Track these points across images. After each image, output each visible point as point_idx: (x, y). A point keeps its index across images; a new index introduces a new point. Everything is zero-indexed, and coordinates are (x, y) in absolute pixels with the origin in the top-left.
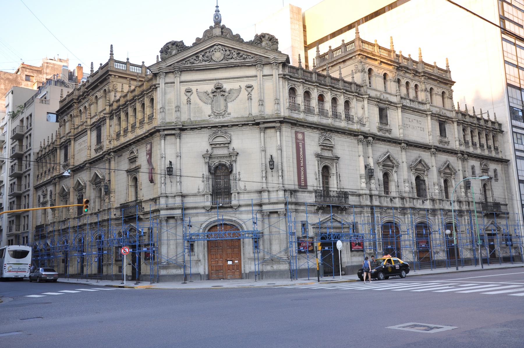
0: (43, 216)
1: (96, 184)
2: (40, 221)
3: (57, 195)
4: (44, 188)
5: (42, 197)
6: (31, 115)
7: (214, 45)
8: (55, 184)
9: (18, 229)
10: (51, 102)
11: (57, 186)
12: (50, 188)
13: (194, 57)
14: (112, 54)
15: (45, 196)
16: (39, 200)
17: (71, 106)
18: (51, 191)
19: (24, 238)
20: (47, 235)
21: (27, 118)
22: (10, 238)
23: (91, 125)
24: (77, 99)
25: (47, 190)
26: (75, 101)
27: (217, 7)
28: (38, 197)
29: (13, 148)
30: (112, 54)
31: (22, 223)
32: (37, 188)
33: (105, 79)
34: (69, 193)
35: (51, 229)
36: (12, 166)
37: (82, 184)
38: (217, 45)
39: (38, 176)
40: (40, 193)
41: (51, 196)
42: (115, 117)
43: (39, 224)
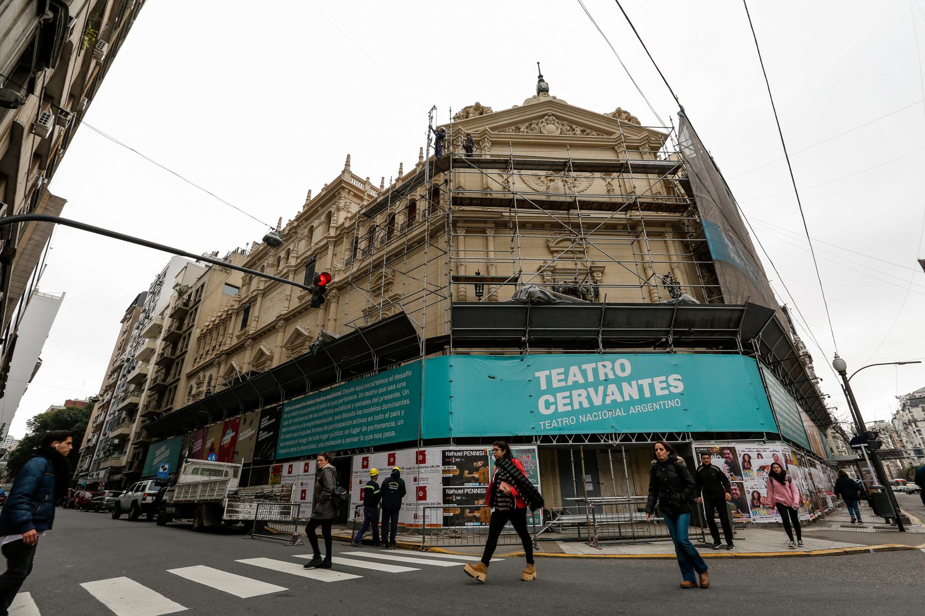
1: (292, 350)
4: (201, 374)
5: (195, 386)
6: (202, 286)
7: (546, 115)
8: (219, 364)
13: (513, 128)
14: (348, 164)
15: (199, 384)
16: (190, 393)
21: (197, 291)
23: (296, 266)
25: (204, 376)
27: (540, 76)
30: (348, 164)
32: (190, 376)
33: (334, 196)
37: (268, 353)
38: (550, 116)
40: (193, 382)
41: (209, 383)
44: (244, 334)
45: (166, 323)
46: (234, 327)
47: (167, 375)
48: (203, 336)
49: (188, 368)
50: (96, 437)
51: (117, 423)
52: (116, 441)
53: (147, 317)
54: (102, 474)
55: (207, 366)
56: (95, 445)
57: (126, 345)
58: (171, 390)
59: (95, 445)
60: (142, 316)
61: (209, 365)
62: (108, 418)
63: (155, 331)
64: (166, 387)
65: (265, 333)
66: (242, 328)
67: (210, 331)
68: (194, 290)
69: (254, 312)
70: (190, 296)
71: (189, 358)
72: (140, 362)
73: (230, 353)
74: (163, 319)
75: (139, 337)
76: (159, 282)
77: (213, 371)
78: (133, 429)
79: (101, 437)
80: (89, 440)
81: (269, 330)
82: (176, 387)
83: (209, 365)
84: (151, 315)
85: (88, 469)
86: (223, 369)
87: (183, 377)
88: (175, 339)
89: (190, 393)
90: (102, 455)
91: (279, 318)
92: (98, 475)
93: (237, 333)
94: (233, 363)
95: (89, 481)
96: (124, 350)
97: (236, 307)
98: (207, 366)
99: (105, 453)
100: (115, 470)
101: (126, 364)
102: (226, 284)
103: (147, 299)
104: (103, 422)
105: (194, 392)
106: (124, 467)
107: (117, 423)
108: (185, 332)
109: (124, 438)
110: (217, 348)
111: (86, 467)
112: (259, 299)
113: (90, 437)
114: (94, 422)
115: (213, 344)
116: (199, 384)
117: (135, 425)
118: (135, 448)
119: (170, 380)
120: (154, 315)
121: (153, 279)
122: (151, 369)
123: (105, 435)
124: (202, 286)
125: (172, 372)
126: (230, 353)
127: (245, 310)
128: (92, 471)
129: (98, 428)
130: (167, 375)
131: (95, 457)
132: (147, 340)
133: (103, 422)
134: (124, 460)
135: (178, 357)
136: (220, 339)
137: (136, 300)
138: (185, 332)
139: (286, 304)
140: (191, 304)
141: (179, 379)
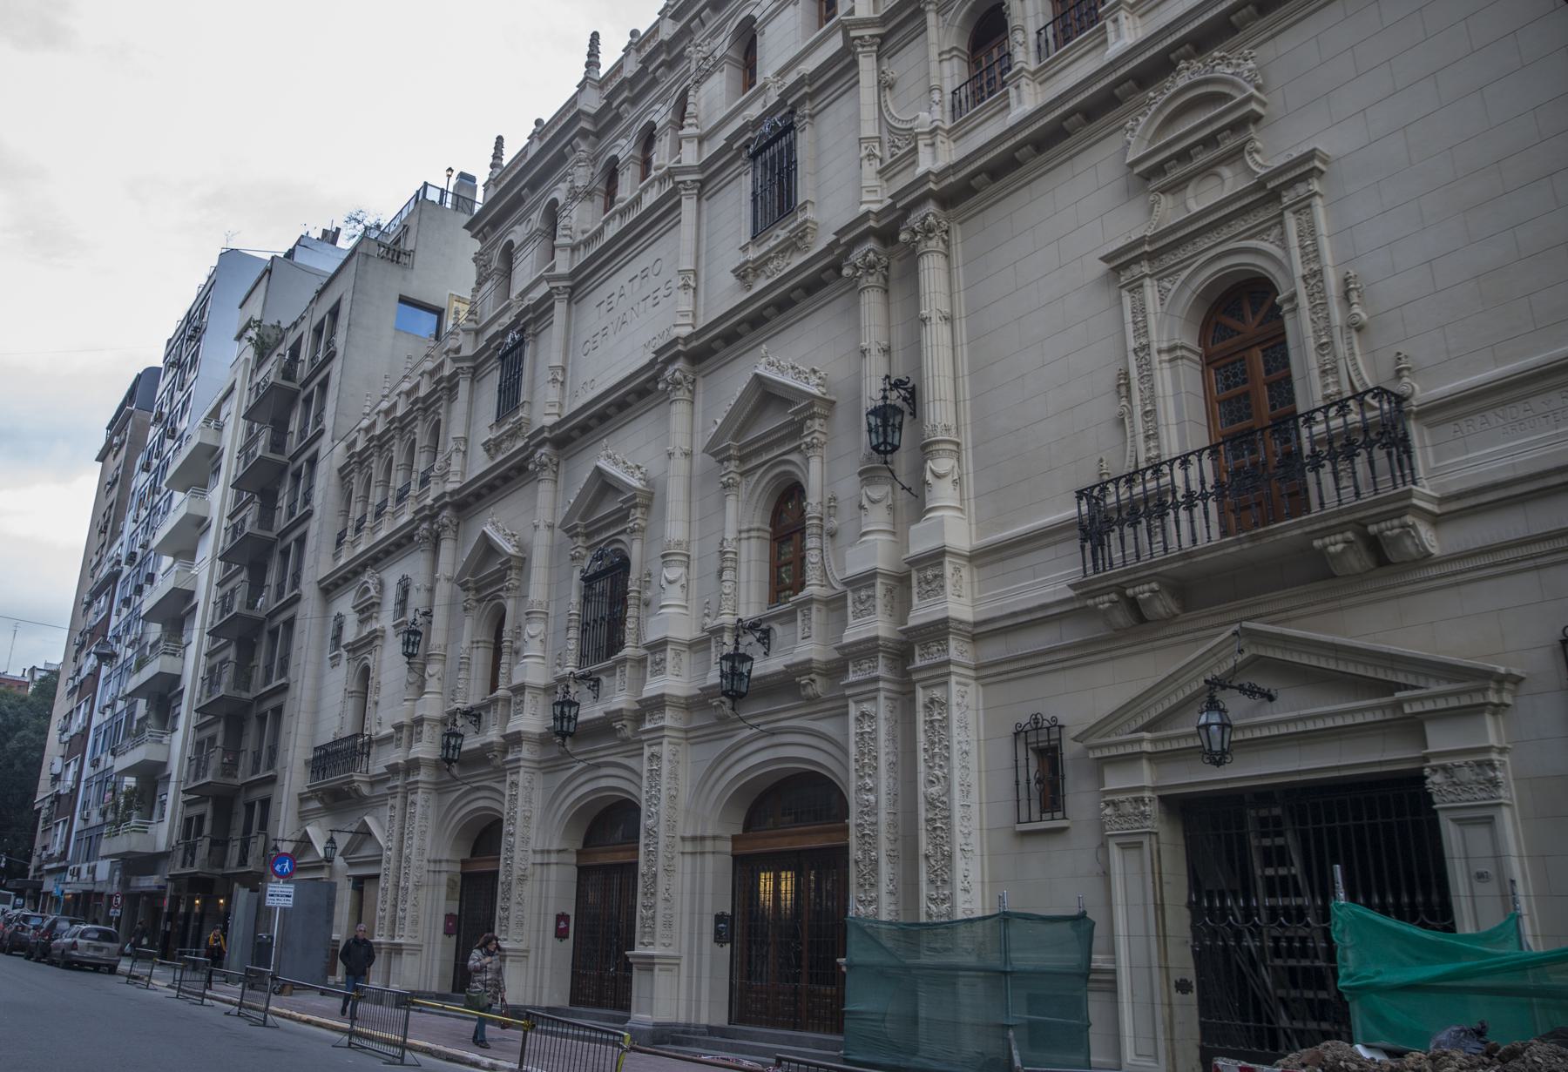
0: (351, 703)
2: (334, 723)
3: (443, 590)
4: (369, 578)
5: (351, 620)
6: (334, 313)
8: (435, 542)
9: (230, 768)
10: (419, 257)
11: (446, 547)
12: (392, 576)
15: (367, 610)
16: (337, 638)
17: (561, 159)
18: (405, 587)
19: (250, 807)
20: (365, 790)
21: (318, 331)
22: (195, 811)
24: (596, 118)
25: (381, 584)
26: (585, 124)
28: (331, 625)
29: (235, 526)
31: (249, 743)
32: (330, 589)
34: (522, 563)
35: (380, 761)
36: (224, 597)
39: (341, 536)
40: (345, 604)
41: (402, 603)
42: (931, 18)
43: (326, 737)
44: (513, 435)
45: (232, 438)
46: (472, 422)
47: (257, 587)
48: (357, 462)
49: (318, 563)
50: (73, 768)
51: (122, 733)
52: (130, 781)
53: (171, 433)
54: (103, 869)
55: (387, 553)
56: (74, 792)
57: (120, 517)
58: (274, 633)
59: (74, 792)
60: (153, 433)
61: (400, 545)
62: (97, 719)
63: (204, 462)
64: (258, 624)
65: (584, 429)
66: (500, 419)
67: (380, 443)
68: (306, 329)
69: (546, 353)
70: (295, 350)
71: (319, 533)
72: (167, 561)
73: (470, 501)
74: (220, 429)
75: (155, 490)
76: (192, 330)
77: (413, 566)
78: (176, 748)
79: (88, 771)
80: (56, 778)
81: (622, 405)
82: (290, 624)
83: (400, 545)
84: (182, 425)
85: (64, 855)
86: (451, 558)
87: (309, 589)
88: (266, 481)
89: (337, 638)
90: (95, 819)
91: (667, 354)
92: (92, 871)
93: (483, 433)
94: (488, 529)
95: (70, 886)
96: (116, 534)
97: (468, 351)
98: (387, 553)
99: (103, 814)
100: (133, 864)
101: (126, 569)
102: (403, 300)
103: (162, 385)
104: (86, 729)
105: (349, 635)
106: (165, 856)
107: (122, 733)
108: (294, 458)
109: (152, 776)
110: (414, 490)
111: (56, 849)
112: (560, 308)
113: (57, 769)
114: (64, 730)
115: (376, 496)
116: (367, 610)
117: (178, 738)
118: (188, 804)
119: (267, 602)
120: (192, 426)
121: (169, 324)
122: (205, 573)
123: (95, 763)
124: (334, 313)
125: (272, 578)
126: (470, 501)
127: (507, 356)
128: (76, 860)
129: (76, 746)
130: (257, 587)
131: (78, 824)
132: (178, 496)
133: (86, 729)
134: (162, 834)
135: (284, 534)
136: (421, 463)
137: (131, 396)
138: (294, 458)
139: (685, 301)
140: (303, 371)
141: (296, 599)
